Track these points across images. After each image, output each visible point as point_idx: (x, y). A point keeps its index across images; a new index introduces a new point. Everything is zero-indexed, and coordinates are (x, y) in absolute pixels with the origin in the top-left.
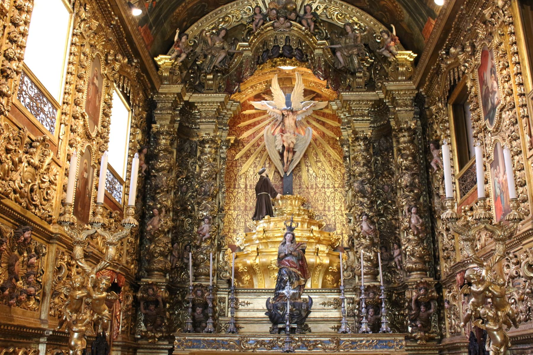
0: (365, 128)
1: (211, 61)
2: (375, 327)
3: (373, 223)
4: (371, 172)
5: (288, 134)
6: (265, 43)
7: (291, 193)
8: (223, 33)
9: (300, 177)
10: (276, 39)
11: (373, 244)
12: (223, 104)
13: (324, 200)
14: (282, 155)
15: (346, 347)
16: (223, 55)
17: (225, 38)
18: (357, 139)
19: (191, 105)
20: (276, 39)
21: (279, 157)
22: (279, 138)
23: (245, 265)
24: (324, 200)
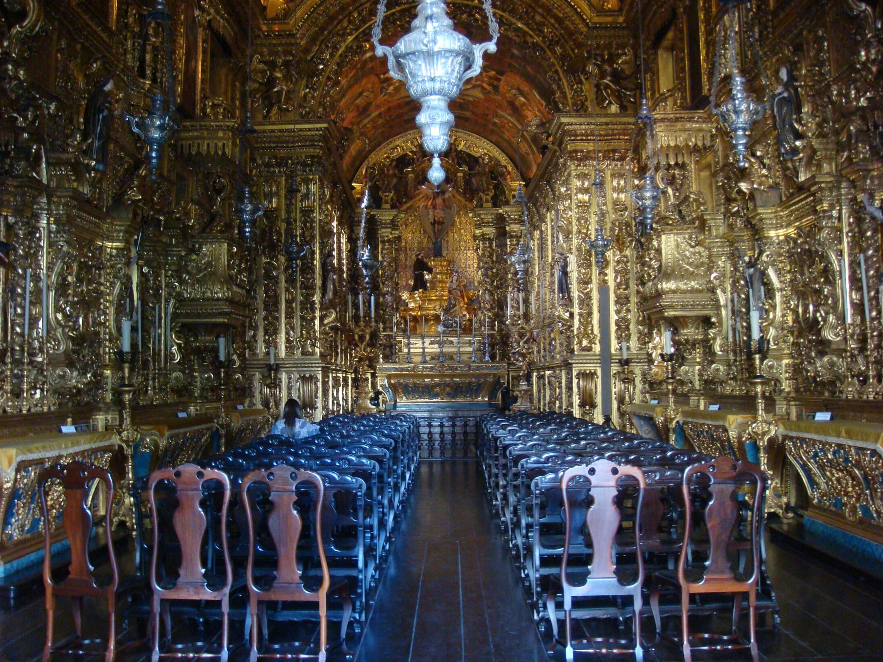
0: (490, 231)
1: (388, 185)
2: (493, 357)
4: (493, 262)
5: (438, 211)
7: (441, 255)
8: (394, 163)
9: (447, 242)
11: (492, 308)
12: (396, 216)
13: (466, 259)
14: (433, 224)
15: (474, 369)
16: (395, 181)
17: (397, 166)
21: (431, 227)
22: (431, 213)
24: (466, 259)
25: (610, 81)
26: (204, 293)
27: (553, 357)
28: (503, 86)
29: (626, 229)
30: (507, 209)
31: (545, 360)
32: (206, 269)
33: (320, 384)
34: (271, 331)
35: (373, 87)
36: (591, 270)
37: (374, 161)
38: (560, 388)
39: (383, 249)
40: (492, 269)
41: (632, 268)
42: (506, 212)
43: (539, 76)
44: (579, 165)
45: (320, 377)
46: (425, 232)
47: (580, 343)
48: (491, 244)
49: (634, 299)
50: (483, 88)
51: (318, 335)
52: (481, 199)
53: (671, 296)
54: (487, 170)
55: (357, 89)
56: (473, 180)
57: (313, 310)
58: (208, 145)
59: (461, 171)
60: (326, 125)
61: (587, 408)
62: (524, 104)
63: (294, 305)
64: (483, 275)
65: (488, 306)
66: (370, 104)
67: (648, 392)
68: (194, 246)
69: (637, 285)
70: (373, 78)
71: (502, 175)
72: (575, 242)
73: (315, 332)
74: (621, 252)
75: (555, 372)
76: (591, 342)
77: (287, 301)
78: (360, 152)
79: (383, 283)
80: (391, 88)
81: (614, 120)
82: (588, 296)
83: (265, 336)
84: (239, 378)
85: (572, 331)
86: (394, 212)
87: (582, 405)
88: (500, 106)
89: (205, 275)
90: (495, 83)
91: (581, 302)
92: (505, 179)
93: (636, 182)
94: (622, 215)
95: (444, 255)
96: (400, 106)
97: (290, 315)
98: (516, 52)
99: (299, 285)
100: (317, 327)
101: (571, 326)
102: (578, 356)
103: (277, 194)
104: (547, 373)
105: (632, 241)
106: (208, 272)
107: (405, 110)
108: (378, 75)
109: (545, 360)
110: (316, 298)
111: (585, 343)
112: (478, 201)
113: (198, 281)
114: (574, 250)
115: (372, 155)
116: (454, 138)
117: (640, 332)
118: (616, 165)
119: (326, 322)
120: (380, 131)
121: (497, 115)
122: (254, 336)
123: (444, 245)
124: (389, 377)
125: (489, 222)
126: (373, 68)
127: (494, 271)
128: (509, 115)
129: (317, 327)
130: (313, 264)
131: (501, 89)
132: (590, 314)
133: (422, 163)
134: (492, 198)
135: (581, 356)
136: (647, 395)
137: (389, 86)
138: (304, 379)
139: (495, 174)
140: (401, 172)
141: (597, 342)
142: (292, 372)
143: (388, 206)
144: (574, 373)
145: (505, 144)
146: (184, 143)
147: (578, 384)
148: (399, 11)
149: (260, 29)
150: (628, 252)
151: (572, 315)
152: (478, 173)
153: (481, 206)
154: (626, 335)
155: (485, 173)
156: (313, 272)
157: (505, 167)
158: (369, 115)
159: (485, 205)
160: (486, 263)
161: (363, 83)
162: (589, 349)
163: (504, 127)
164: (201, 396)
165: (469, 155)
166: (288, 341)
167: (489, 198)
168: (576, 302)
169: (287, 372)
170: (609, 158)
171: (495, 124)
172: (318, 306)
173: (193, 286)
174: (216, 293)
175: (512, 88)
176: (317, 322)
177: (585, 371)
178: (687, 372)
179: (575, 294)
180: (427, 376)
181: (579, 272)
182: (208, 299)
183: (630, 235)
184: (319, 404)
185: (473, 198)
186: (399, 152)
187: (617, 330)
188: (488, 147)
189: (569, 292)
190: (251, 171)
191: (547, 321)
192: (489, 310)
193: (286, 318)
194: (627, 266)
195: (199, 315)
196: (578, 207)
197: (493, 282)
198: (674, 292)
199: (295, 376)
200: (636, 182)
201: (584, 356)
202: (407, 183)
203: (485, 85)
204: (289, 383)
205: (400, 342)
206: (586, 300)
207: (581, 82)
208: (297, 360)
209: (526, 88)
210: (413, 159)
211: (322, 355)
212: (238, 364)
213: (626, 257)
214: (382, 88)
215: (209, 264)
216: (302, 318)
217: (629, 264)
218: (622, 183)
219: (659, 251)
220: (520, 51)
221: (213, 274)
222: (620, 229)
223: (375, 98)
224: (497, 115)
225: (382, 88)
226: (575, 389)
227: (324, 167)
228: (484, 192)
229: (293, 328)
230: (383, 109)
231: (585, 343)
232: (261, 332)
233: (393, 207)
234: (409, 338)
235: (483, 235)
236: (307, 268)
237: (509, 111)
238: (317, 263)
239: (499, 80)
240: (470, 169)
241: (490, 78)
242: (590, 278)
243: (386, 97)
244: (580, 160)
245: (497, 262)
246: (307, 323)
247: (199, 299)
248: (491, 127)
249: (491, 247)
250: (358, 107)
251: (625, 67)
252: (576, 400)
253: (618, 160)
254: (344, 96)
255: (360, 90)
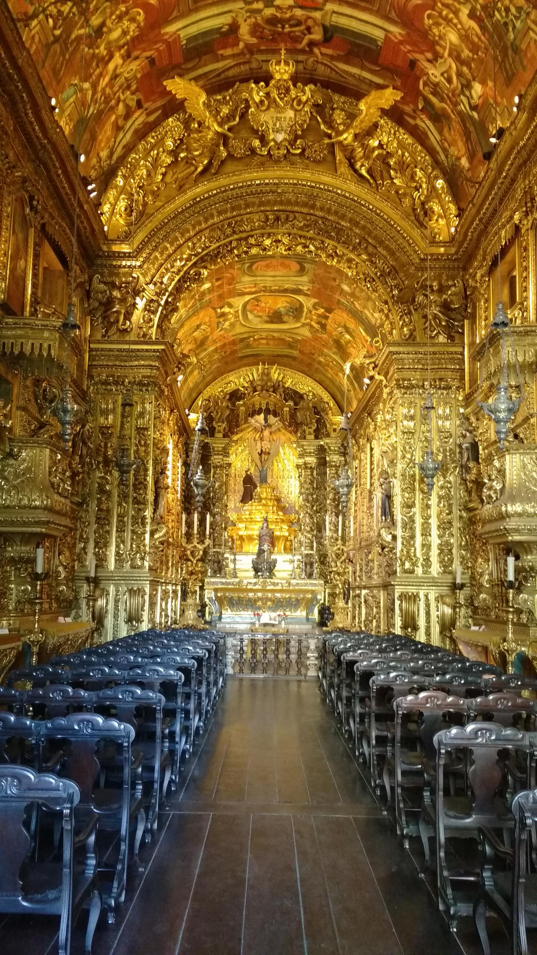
0: (312, 460)
1: (221, 416)
3: (312, 518)
4: (313, 488)
6: (254, 406)
8: (228, 397)
9: (272, 470)
10: (260, 404)
11: (312, 530)
14: (260, 454)
16: (228, 412)
17: (230, 400)
18: (306, 468)
19: (207, 443)
20: (260, 404)
21: (258, 456)
22: (259, 443)
23: (238, 534)
25: (440, 312)
26: (20, 500)
27: (370, 578)
28: (330, 324)
29: (450, 455)
30: (328, 441)
31: (361, 579)
32: (24, 474)
33: (147, 597)
34: (102, 543)
35: (210, 321)
36: (415, 495)
37: (209, 394)
38: (378, 607)
39: (215, 473)
40: (312, 495)
41: (456, 494)
42: (327, 444)
43: (366, 311)
44: (406, 393)
45: (147, 590)
46: (253, 461)
47: (403, 564)
48: (312, 472)
49: (457, 524)
50: (312, 326)
51: (147, 549)
52: (304, 431)
53: (517, 519)
54: (311, 405)
55: (195, 321)
56: (298, 414)
57: (144, 524)
58: (33, 344)
59: (287, 406)
60: (163, 347)
61: (409, 630)
62: (349, 342)
63: (126, 519)
64: (304, 500)
65: (308, 529)
66: (206, 338)
67: (471, 617)
68: (12, 450)
69: (460, 511)
70: (211, 311)
71: (324, 410)
72: (400, 466)
73: (144, 546)
74: (444, 478)
75: (372, 591)
76: (414, 564)
77: (118, 516)
78: (196, 385)
79: (214, 505)
80: (227, 323)
81: (441, 349)
82: (412, 520)
83: (95, 548)
84: (63, 590)
85: (395, 554)
86: (226, 440)
87: (404, 627)
88: (326, 345)
89: (23, 481)
90: (323, 321)
91: (405, 526)
92: (327, 414)
93: (462, 410)
94: (446, 442)
95: (269, 481)
96: (234, 343)
97: (121, 530)
98: (346, 288)
99: (131, 500)
100: (147, 541)
101: (393, 548)
102: (400, 578)
103: (114, 411)
104: (364, 592)
105: (456, 467)
106: (27, 478)
107: (239, 346)
108: (214, 309)
109: (361, 579)
110: (148, 513)
111: (407, 565)
112: (301, 434)
113: (14, 487)
114: (398, 475)
115: (208, 389)
116: (282, 375)
117: (463, 557)
118: (442, 394)
119: (156, 536)
120: (215, 366)
121: (322, 354)
122: (84, 548)
123: (269, 473)
124: (216, 590)
125: (310, 453)
126: (210, 301)
127: (314, 496)
128: (334, 353)
129: (147, 541)
130: (145, 480)
131: (328, 327)
132: (413, 537)
133: (252, 397)
134: (314, 431)
135: (402, 578)
136: (470, 620)
137: (225, 321)
138: (131, 592)
139: (318, 411)
140: (234, 404)
141: (419, 565)
142: (120, 585)
143: (221, 435)
144: (397, 595)
145: (328, 382)
146: (6, 341)
147: (400, 606)
148: (237, 240)
149: (101, 249)
150: (451, 478)
151: (394, 538)
152: (303, 408)
153: (305, 438)
154: (449, 559)
155: (308, 409)
156: (146, 488)
157: (328, 403)
158: (206, 350)
159: (308, 437)
160: (307, 489)
161: (201, 315)
162: (412, 572)
163: (328, 365)
164: (16, 609)
165: (296, 392)
166: (118, 554)
167: (312, 431)
168: (399, 524)
169: (115, 585)
170: (435, 387)
171: (320, 363)
172: (149, 521)
173: (8, 492)
174: (34, 501)
175: (339, 325)
176: (147, 536)
177: (408, 593)
178: (526, 601)
179: (399, 517)
180: (251, 590)
181: (403, 496)
182: (25, 507)
183: (454, 462)
184: (145, 616)
185: (298, 430)
186: (232, 387)
187: (439, 554)
188: (312, 384)
189: (392, 516)
190: (88, 388)
191: (363, 544)
192: (308, 532)
193: (117, 531)
194: (450, 492)
195: (13, 523)
196: (404, 433)
197: (313, 506)
198: (520, 515)
199: (123, 589)
200: (462, 410)
201: (407, 578)
202: (238, 415)
203: (313, 323)
204: (117, 595)
205: (227, 558)
206: (409, 525)
207: (410, 313)
208: (127, 572)
209: (352, 325)
210: (245, 394)
211: (151, 569)
212: (63, 576)
213: (450, 483)
214: (218, 323)
215: (28, 470)
216: (133, 532)
217: (452, 490)
218: (448, 411)
219: (501, 472)
220: (350, 288)
221: (33, 480)
222: (445, 456)
223: (211, 333)
224: (322, 354)
225: (218, 323)
226: (397, 611)
227: (160, 388)
228: (307, 425)
229: (123, 542)
230: (218, 345)
231: (407, 565)
232: (91, 545)
233: (224, 436)
234: (235, 554)
235: (305, 464)
236: (140, 485)
237: (335, 350)
238: (150, 479)
239: (327, 318)
240: (296, 404)
241: (319, 316)
242: (414, 502)
243: (222, 332)
244: (407, 388)
245: (317, 489)
246: (138, 536)
247: (14, 507)
248: (317, 366)
249: (312, 474)
250: (195, 340)
251: (454, 298)
252: (398, 622)
253: (444, 388)
254: (182, 326)
255: (198, 323)
